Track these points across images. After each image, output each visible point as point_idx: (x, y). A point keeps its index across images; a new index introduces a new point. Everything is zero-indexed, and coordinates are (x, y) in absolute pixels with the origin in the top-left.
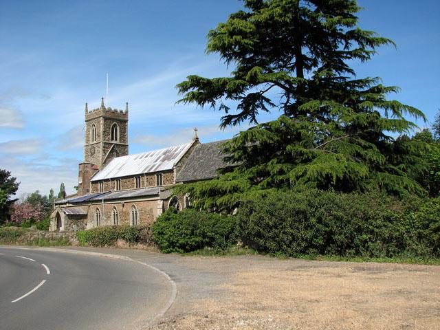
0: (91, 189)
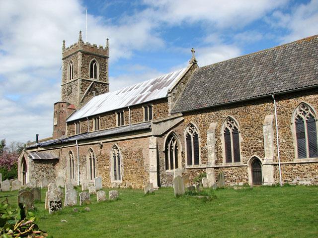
0: (67, 131)
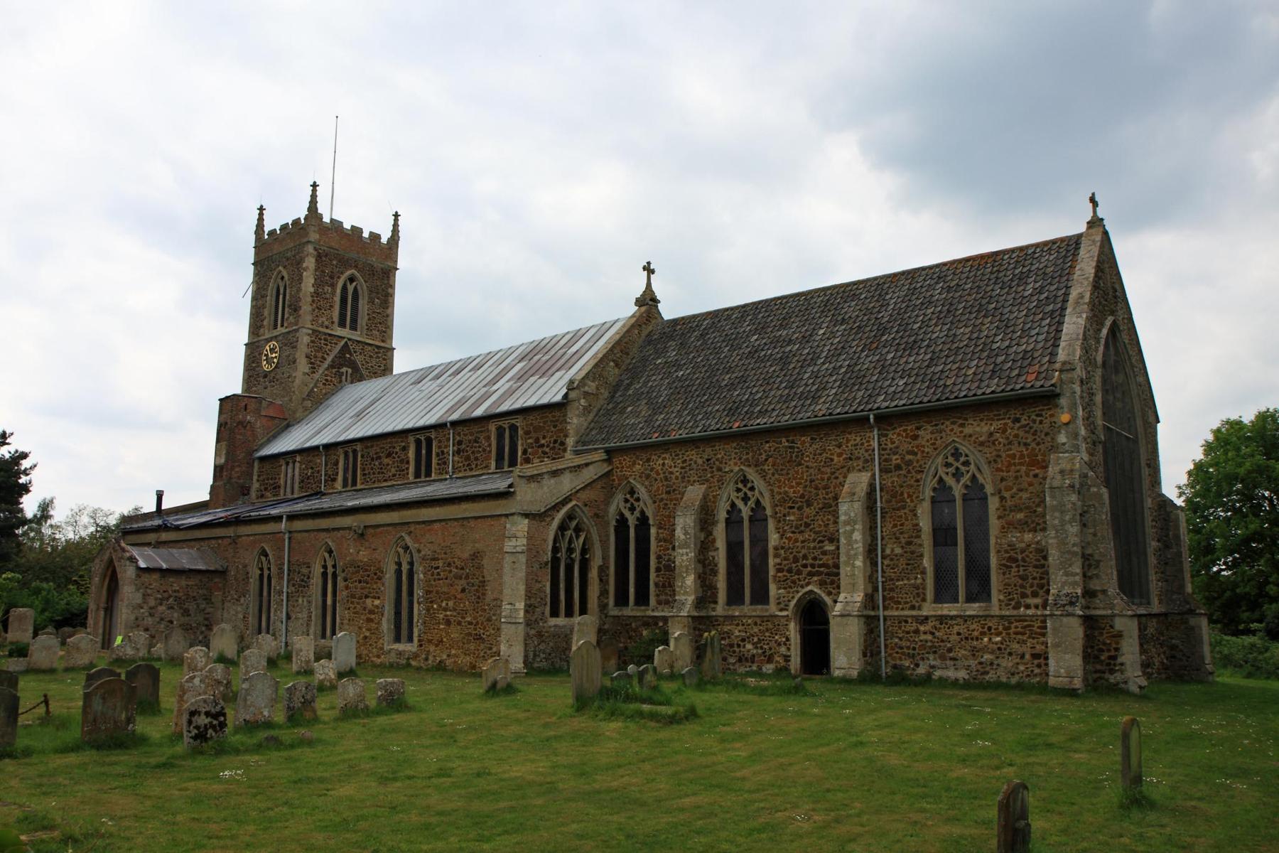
0: (256, 485)
